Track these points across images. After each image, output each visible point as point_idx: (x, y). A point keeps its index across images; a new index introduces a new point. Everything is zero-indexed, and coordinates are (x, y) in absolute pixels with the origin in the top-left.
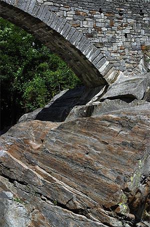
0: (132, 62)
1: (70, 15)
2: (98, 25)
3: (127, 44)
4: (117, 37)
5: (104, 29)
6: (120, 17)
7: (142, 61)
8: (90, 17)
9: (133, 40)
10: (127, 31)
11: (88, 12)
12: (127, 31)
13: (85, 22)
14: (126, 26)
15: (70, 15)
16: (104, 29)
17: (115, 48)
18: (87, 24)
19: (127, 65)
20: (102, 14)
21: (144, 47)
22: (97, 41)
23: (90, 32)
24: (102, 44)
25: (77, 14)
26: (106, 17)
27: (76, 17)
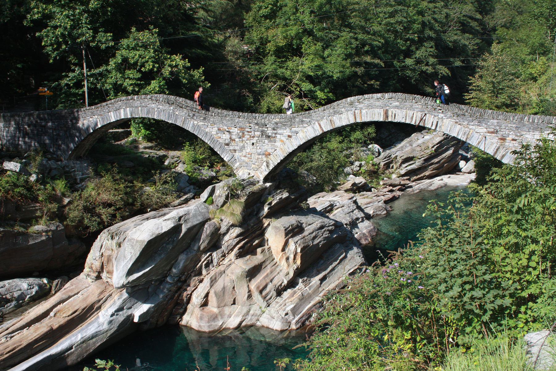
0: (256, 164)
1: (214, 131)
2: (233, 137)
3: (254, 150)
4: (246, 145)
5: (237, 140)
6: (249, 130)
7: (265, 164)
8: (228, 131)
9: (258, 148)
10: (254, 141)
11: (226, 128)
12: (254, 141)
13: (224, 135)
14: (254, 137)
15: (214, 131)
16: (237, 140)
17: (244, 153)
18: (226, 136)
19: (253, 166)
20: (236, 129)
21: (267, 153)
22: (231, 148)
23: (227, 142)
24: (235, 151)
25: (219, 129)
26: (239, 131)
27: (218, 132)
